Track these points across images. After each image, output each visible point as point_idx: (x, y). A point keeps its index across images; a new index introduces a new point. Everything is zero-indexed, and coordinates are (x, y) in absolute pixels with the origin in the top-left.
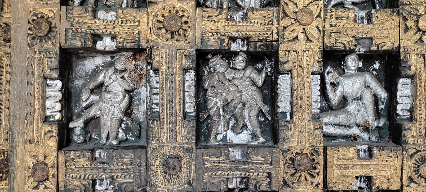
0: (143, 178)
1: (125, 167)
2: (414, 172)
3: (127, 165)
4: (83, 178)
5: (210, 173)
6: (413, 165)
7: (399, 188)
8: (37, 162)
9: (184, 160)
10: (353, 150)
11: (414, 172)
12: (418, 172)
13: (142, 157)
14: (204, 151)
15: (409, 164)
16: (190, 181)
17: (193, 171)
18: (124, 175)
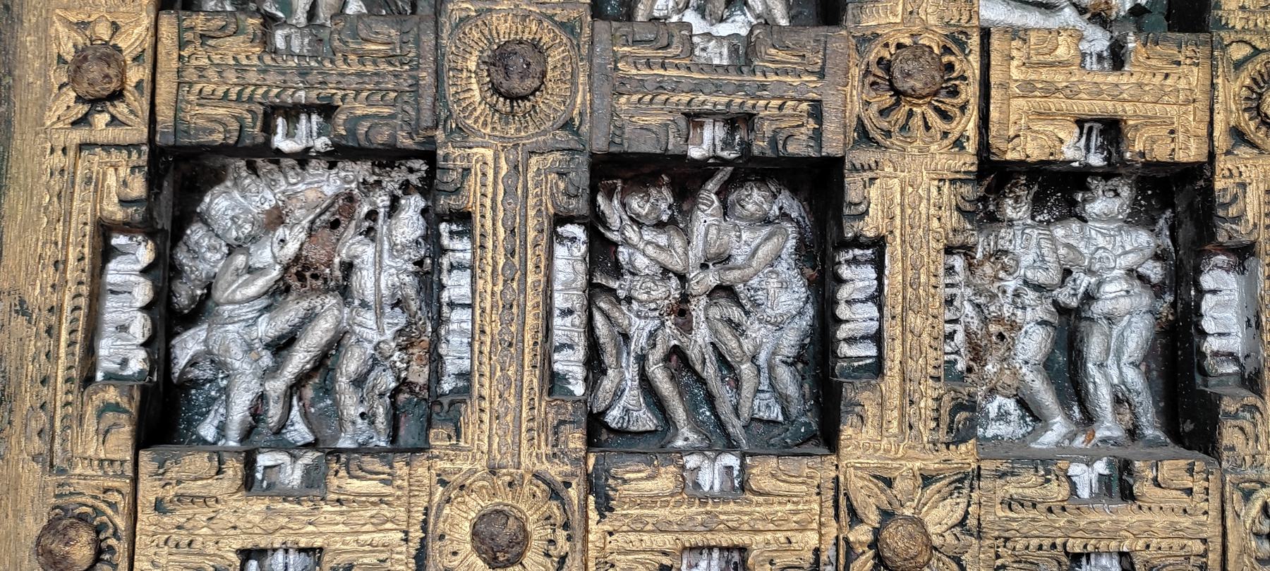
0: (427, 102)
1: (370, 68)
2: (1245, 110)
3: (375, 63)
4: (234, 97)
5: (635, 98)
6: (1245, 93)
7: (1204, 159)
8: (88, 42)
9: (555, 57)
10: (1069, 40)
11: (1245, 110)
12: (1259, 114)
13: (424, 38)
14: (616, 29)
15: (1232, 89)
16: (572, 119)
17: (581, 88)
18: (365, 94)
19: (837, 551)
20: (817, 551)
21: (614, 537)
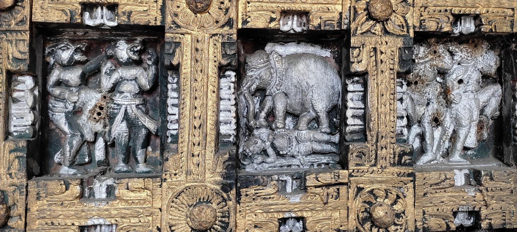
19: (350, 13)
20: (341, 14)
21: (250, 5)
